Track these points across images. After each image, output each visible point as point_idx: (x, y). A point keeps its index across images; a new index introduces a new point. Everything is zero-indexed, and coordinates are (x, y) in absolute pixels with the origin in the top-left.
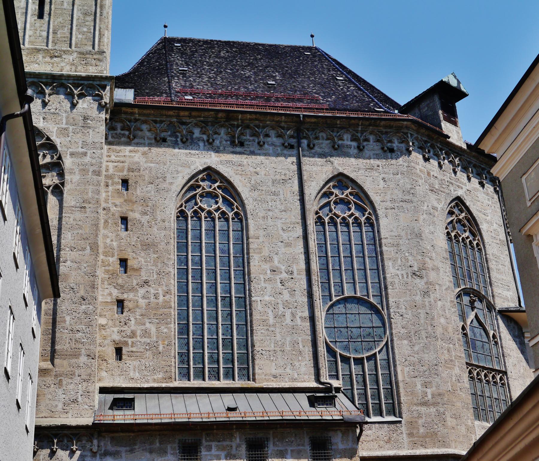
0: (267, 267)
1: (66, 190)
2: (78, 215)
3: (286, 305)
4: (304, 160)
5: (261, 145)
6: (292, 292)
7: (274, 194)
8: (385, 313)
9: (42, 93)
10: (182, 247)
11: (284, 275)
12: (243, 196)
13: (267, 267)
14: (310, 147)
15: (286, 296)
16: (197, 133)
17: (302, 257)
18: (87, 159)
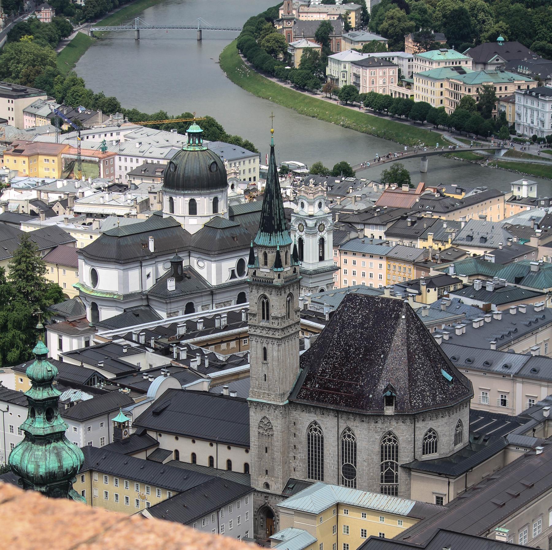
2: (277, 443)
6: (334, 461)
18: (278, 428)
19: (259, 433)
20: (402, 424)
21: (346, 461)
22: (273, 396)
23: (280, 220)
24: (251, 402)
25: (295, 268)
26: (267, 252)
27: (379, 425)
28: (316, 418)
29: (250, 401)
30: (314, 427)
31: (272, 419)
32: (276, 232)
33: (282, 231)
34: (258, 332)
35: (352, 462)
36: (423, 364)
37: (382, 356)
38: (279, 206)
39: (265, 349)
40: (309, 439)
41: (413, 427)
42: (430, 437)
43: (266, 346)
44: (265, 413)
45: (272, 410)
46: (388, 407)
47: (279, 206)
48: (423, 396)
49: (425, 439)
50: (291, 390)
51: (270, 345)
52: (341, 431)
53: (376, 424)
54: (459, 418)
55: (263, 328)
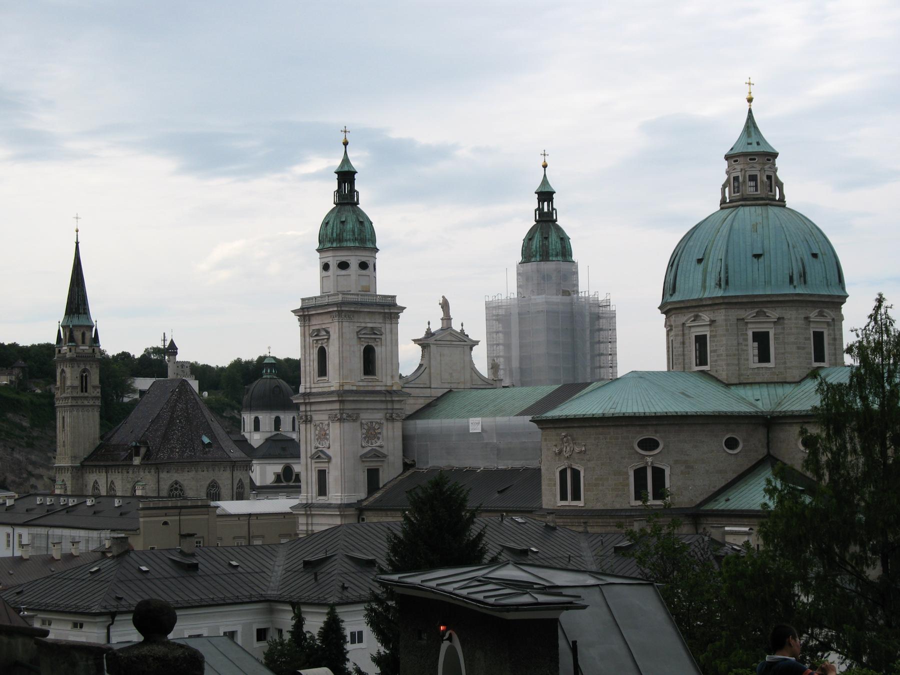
20: (148, 474)
23: (78, 305)
25: (94, 349)
27: (131, 475)
28: (96, 478)
32: (74, 314)
33: (80, 314)
36: (182, 427)
38: (78, 293)
39: (63, 418)
41: (157, 477)
42: (176, 489)
46: (136, 458)
47: (78, 293)
48: (172, 452)
49: (171, 490)
50: (85, 456)
52: (109, 486)
53: (128, 474)
54: (212, 478)
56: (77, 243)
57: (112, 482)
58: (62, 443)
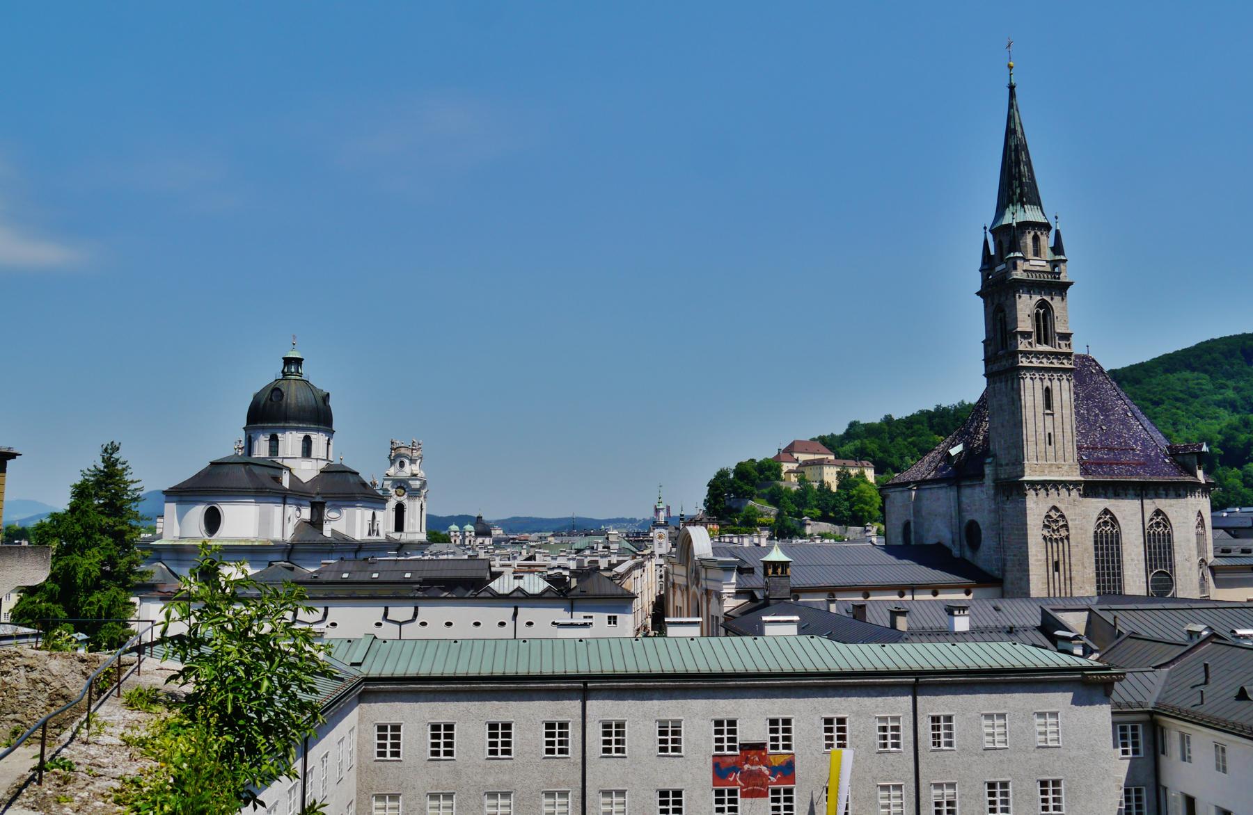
0: (1129, 558)
1: (1071, 537)
2: (1076, 550)
3: (1137, 576)
4: (1144, 501)
5: (1126, 495)
6: (1139, 570)
7: (1132, 521)
8: (1174, 578)
9: (1058, 489)
10: (1096, 549)
11: (1136, 562)
12: (1120, 523)
13: (1129, 558)
14: (1146, 495)
15: (1137, 572)
16: (1101, 491)
17: (1143, 553)
18: (1077, 522)
19: (1045, 538)
21: (1156, 568)
22: (1066, 468)
24: (1033, 484)
26: (1039, 233)
29: (1029, 482)
30: (1108, 519)
31: (1067, 508)
34: (1036, 363)
35: (1166, 567)
37: (1129, 414)
39: (1048, 392)
40: (1096, 542)
43: (1049, 384)
44: (1054, 498)
45: (1064, 492)
51: (1056, 383)
55: (1046, 355)
56: (1012, 88)
57: (1158, 512)
58: (1042, 437)
